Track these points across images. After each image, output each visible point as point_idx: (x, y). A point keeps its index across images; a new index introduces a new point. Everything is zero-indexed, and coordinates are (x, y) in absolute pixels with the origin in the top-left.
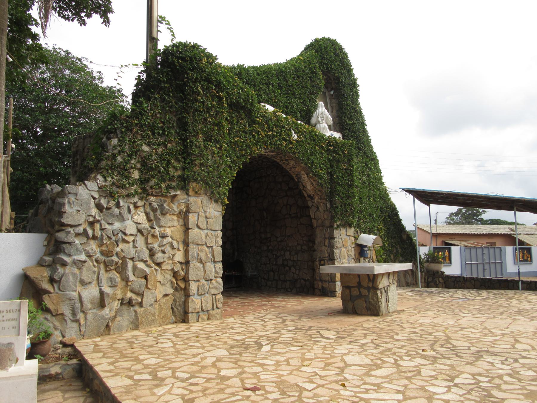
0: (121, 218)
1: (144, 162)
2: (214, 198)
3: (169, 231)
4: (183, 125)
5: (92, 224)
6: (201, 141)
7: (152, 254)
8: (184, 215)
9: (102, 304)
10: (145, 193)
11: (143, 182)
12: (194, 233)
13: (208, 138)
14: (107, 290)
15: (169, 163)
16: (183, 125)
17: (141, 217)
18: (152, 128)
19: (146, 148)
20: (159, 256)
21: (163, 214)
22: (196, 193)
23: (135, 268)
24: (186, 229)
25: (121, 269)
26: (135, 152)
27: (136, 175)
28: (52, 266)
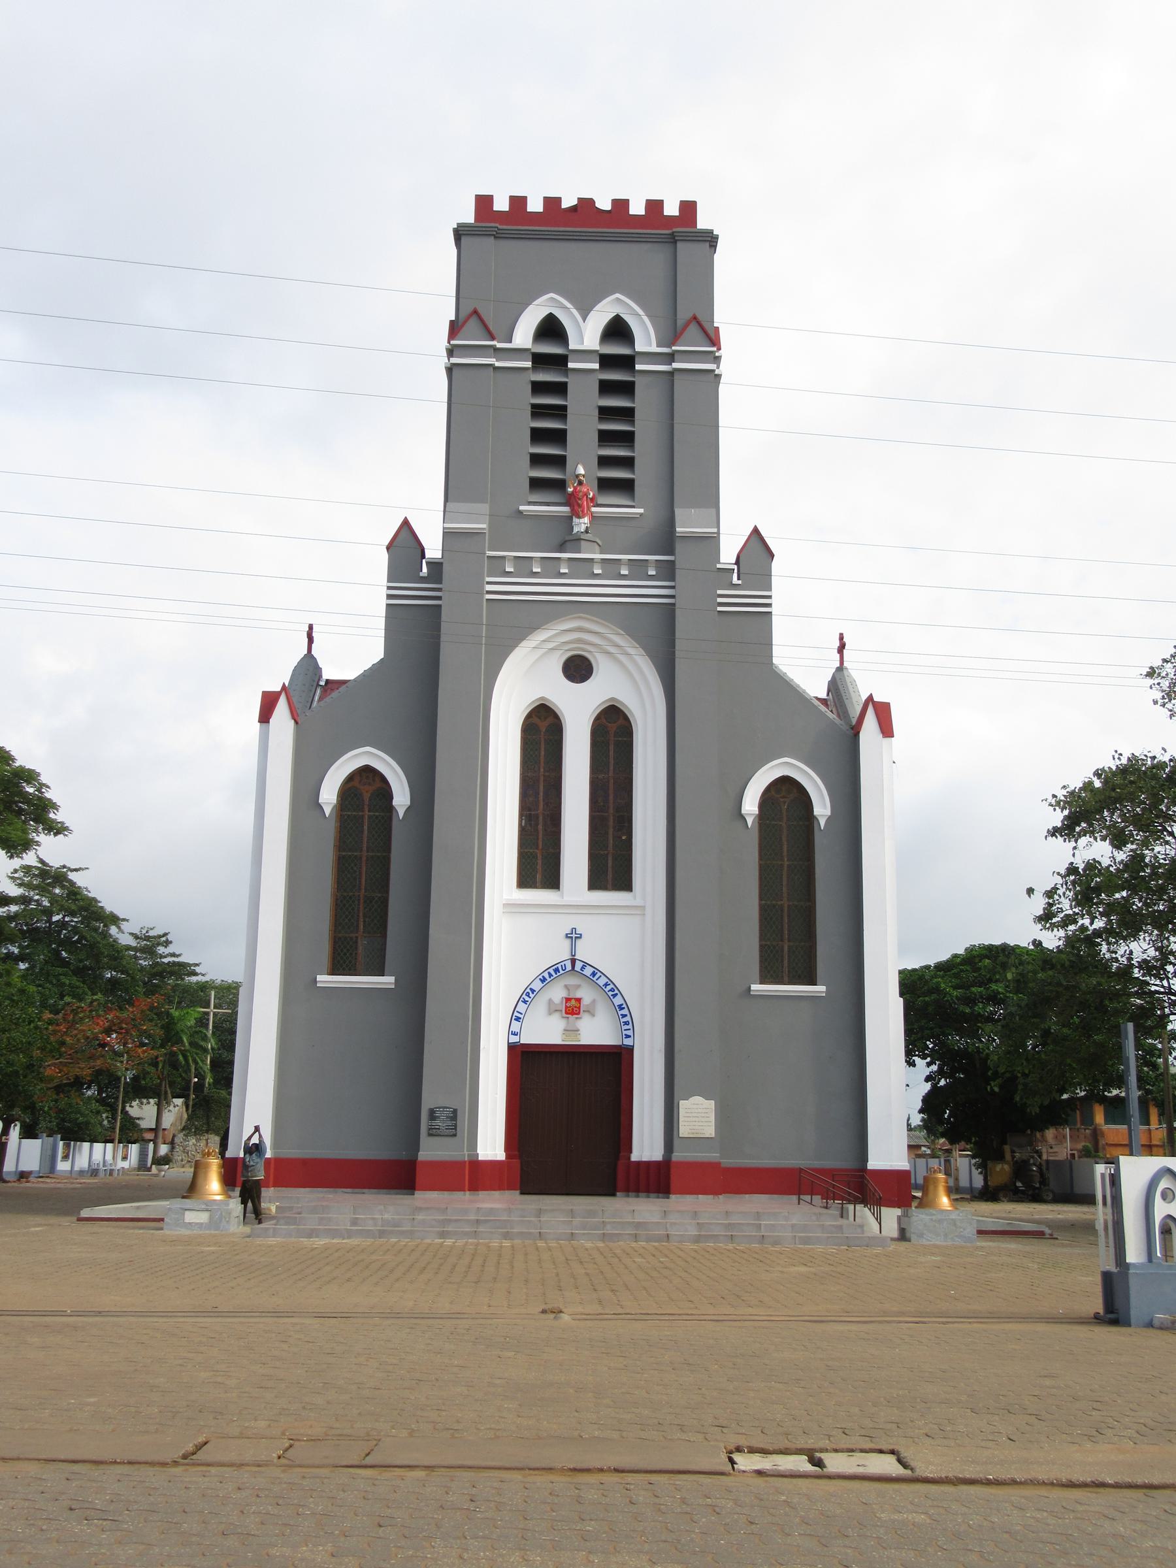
0: (188, 1141)
1: (196, 1128)
2: (217, 1134)
3: (202, 1144)
4: (208, 1116)
5: (181, 1142)
6: (213, 1119)
7: (196, 1150)
8: (207, 1140)
9: (182, 1161)
10: (195, 1135)
11: (195, 1132)
12: (209, 1144)
13: (216, 1118)
14: (183, 1157)
15: (203, 1127)
16: (208, 1116)
17: (194, 1141)
18: (199, 1117)
19: (197, 1123)
20: (198, 1151)
21: (200, 1140)
22: (211, 1134)
23: (191, 1153)
24: (207, 1144)
25: (188, 1153)
26: (193, 1124)
27: (193, 1130)
28: (172, 1152)
